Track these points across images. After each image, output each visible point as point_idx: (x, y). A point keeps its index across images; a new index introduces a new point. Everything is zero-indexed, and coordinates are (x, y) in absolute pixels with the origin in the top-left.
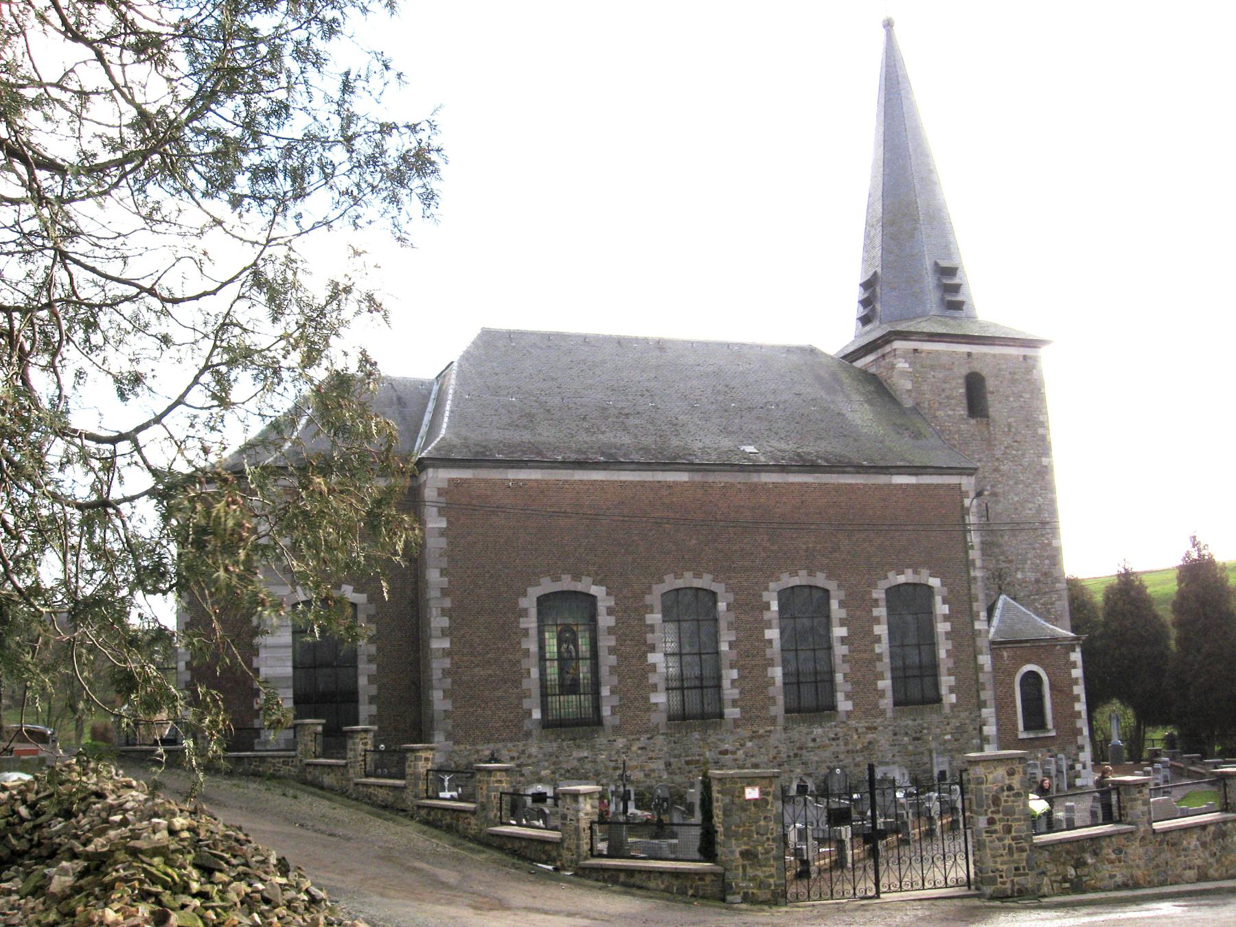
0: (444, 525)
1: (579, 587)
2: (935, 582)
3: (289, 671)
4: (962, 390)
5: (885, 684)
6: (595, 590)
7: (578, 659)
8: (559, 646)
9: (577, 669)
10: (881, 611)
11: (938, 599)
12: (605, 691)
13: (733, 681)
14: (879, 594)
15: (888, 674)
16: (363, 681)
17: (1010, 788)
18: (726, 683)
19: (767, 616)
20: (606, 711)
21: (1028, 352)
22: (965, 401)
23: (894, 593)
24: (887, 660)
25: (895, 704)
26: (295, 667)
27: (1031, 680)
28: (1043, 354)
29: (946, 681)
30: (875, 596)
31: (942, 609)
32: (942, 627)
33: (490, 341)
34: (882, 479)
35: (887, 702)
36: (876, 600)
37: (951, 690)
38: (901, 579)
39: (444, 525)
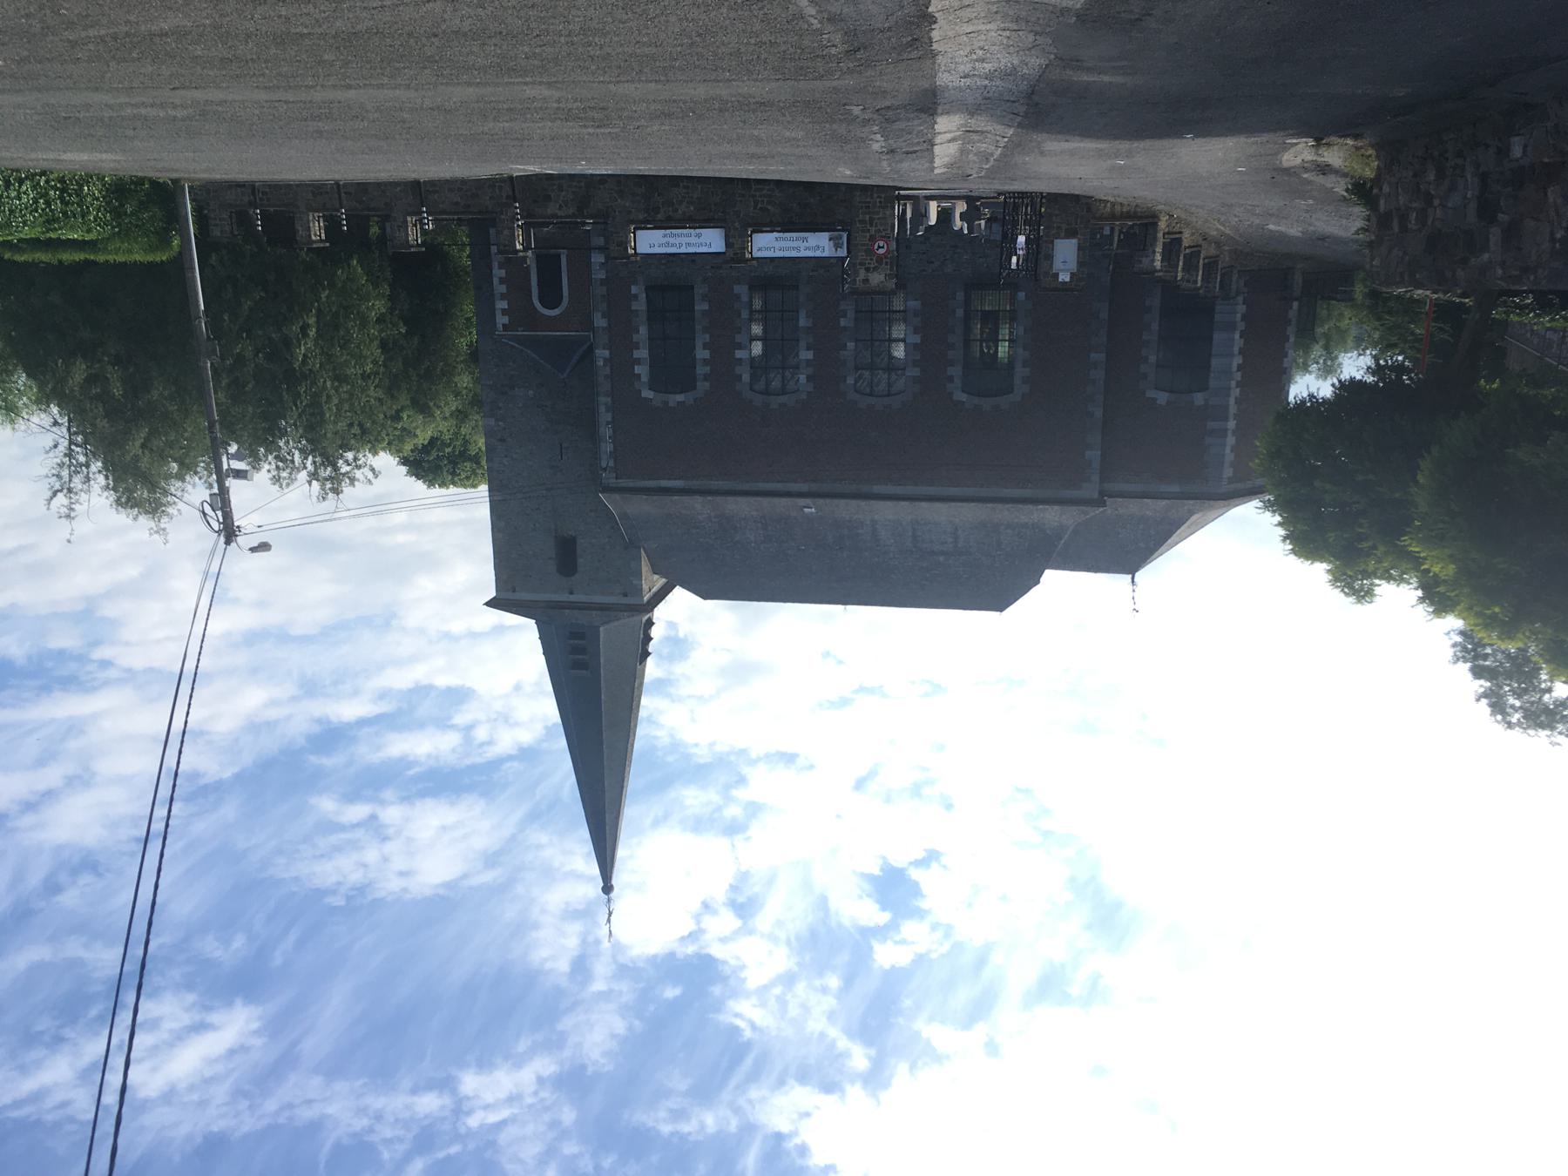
0: (1088, 453)
1: (976, 400)
2: (647, 394)
3: (1216, 336)
4: (580, 561)
5: (701, 307)
6: (964, 397)
7: (981, 341)
8: (996, 351)
9: (982, 332)
10: (701, 370)
11: (645, 378)
12: (960, 313)
13: (845, 316)
14: (703, 386)
15: (698, 315)
16: (1155, 326)
17: (867, 270)
18: (851, 314)
19: (810, 371)
20: (960, 296)
21: (511, 596)
22: (579, 551)
23: (688, 385)
24: (698, 327)
25: (692, 287)
26: (1211, 338)
27: (551, 299)
28: (492, 593)
29: (640, 305)
30: (707, 384)
31: (642, 370)
32: (642, 353)
33: (1001, 610)
34: (814, 487)
35: (700, 290)
36: (705, 379)
37: (636, 297)
38: (680, 398)
39: (1088, 453)
